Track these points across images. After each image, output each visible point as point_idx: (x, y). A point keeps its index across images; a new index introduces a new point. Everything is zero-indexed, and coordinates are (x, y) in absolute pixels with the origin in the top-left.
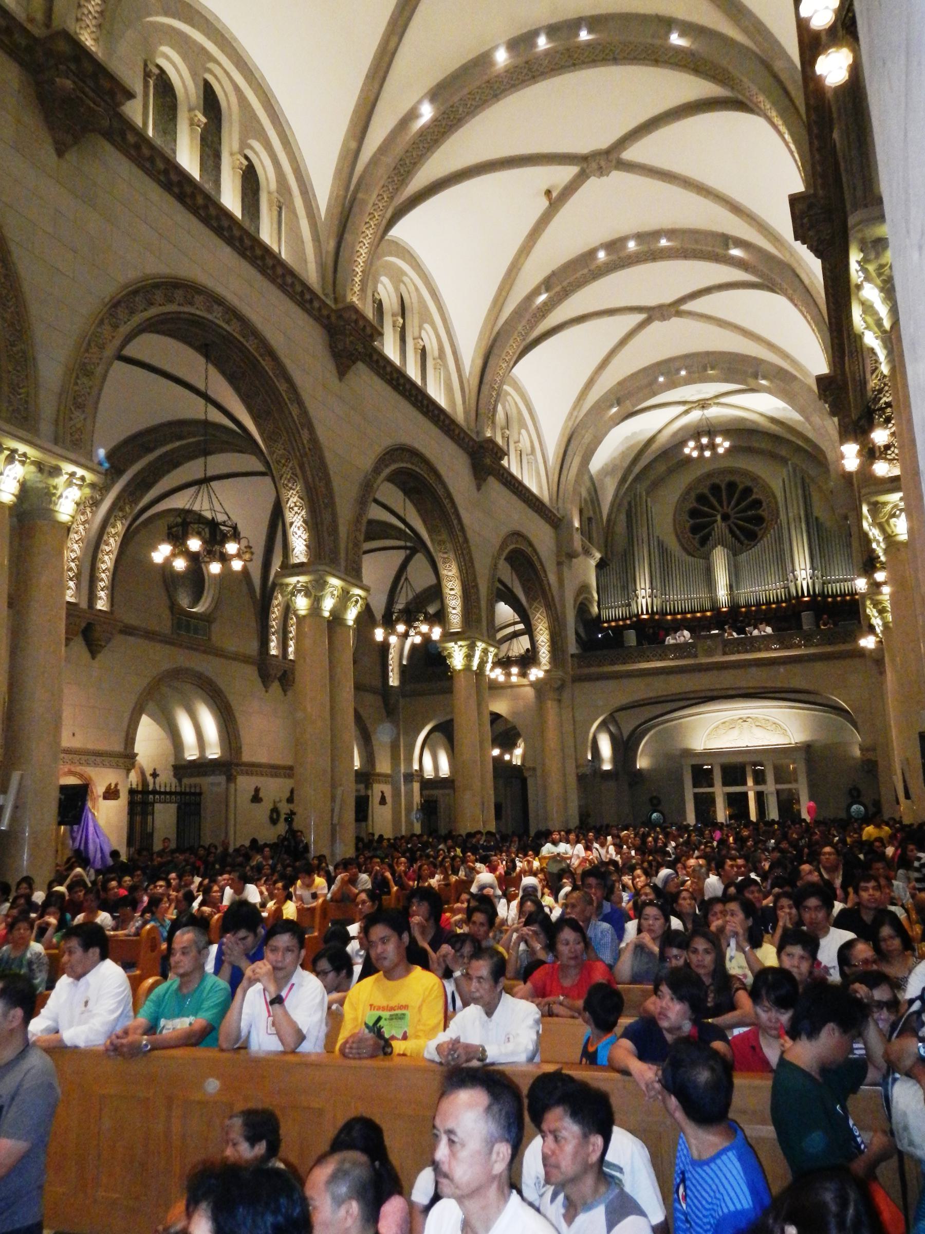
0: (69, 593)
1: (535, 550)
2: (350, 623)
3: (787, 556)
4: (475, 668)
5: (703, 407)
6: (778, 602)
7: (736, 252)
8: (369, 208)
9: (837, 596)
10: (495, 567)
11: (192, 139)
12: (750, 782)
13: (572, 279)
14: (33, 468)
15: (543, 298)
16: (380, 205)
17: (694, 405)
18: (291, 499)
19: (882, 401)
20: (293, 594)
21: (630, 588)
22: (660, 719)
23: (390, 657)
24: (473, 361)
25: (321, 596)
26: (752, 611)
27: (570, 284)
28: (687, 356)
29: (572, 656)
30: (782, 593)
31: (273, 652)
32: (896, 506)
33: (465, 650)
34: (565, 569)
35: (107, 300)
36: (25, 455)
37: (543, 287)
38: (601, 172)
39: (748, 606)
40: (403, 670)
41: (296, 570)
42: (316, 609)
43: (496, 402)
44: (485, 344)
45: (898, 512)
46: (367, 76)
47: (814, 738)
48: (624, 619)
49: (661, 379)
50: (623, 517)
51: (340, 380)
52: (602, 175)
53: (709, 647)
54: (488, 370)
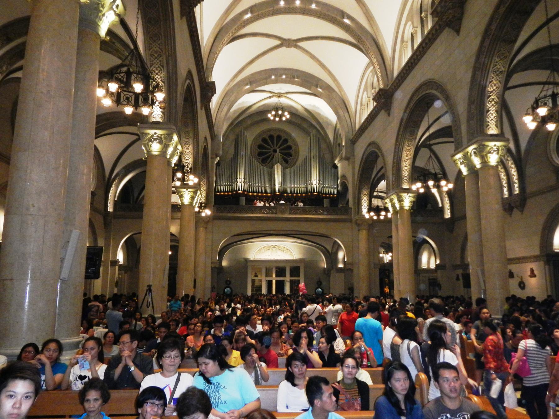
3: (308, 172)
5: (279, 97)
6: (301, 194)
7: (346, 21)
9: (327, 194)
12: (274, 276)
13: (263, 11)
15: (249, 15)
19: (491, 98)
23: (110, 195)
24: (208, 39)
25: (169, 145)
26: (293, 196)
28: (286, 69)
30: (304, 190)
32: (492, 148)
33: (191, 194)
37: (249, 10)
39: (288, 193)
40: (116, 203)
41: (155, 126)
42: (163, 152)
44: (217, 30)
45: (492, 151)
47: (304, 257)
48: (228, 192)
53: (283, 209)
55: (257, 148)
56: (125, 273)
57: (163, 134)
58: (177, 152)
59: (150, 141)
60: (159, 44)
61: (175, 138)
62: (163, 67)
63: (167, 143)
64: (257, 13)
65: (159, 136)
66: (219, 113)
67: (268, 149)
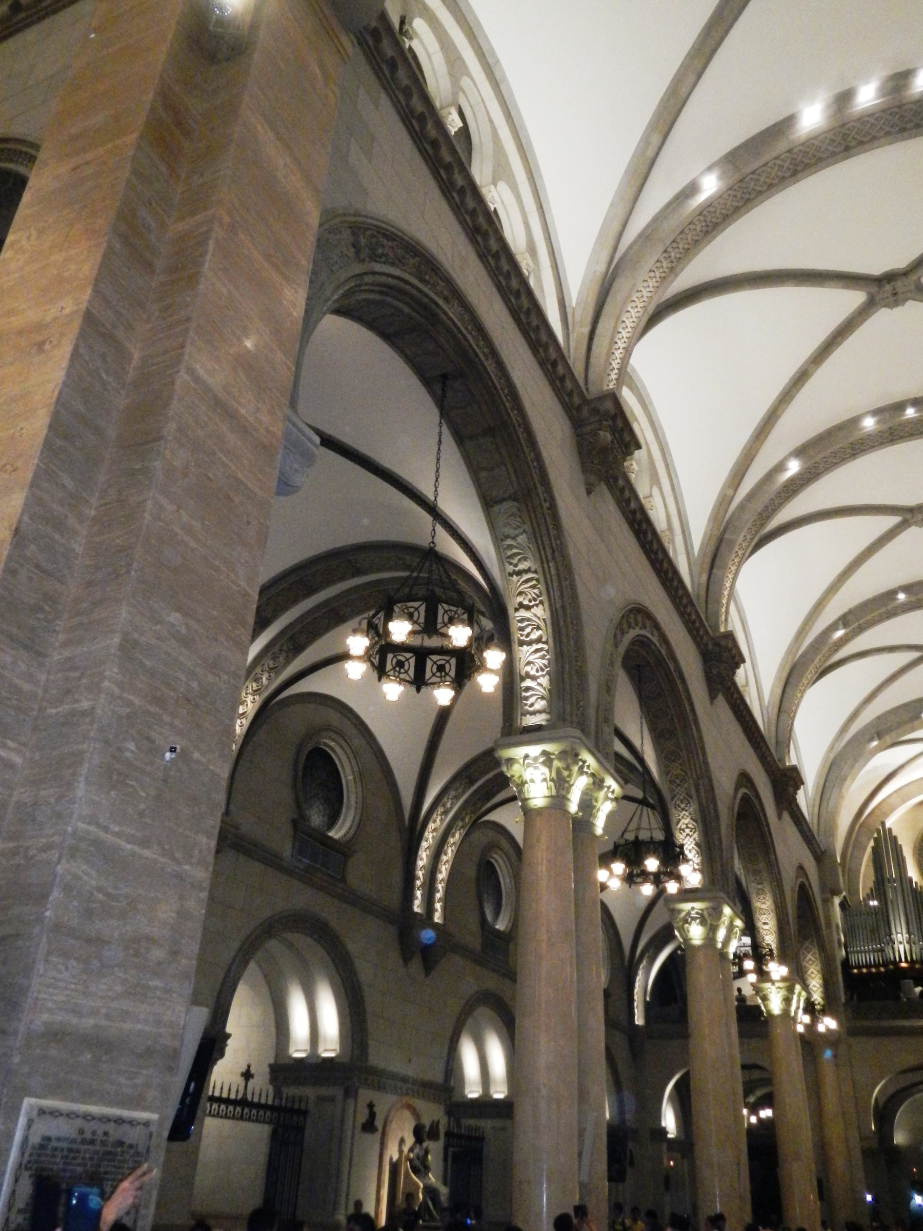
2: (731, 957)
8: (736, 549)
14: (591, 780)
15: (840, 633)
18: (683, 821)
21: (882, 932)
23: (636, 991)
24: (772, 691)
29: (845, 1005)
33: (783, 993)
37: (840, 622)
40: (648, 1007)
42: (710, 939)
44: (785, 674)
48: (877, 966)
51: (712, 703)
54: (784, 700)
57: (706, 909)
58: (735, 931)
59: (686, 922)
60: (681, 765)
61: (727, 911)
62: (691, 798)
63: (715, 924)
64: (857, 623)
65: (700, 912)
66: (824, 804)
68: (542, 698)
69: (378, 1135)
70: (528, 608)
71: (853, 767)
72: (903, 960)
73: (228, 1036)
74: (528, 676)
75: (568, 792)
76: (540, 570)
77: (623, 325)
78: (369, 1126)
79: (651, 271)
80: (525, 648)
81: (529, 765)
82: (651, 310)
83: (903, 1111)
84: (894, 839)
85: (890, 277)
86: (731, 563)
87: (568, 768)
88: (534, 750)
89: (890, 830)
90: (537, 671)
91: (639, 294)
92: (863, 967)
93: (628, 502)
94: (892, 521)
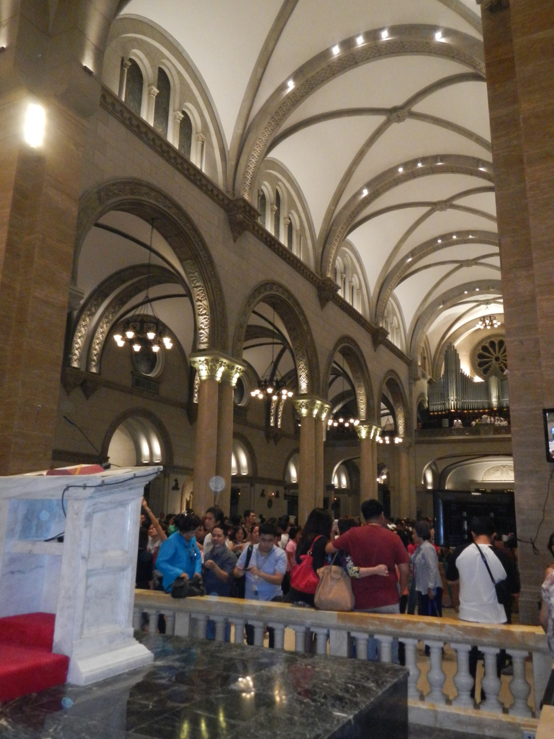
0: (195, 399)
1: (399, 378)
4: (371, 438)
8: (338, 234)
10: (381, 389)
11: (272, 218)
13: (425, 251)
14: (226, 367)
16: (342, 232)
17: (482, 303)
20: (300, 407)
22: (458, 464)
24: (375, 289)
27: (424, 253)
31: (272, 425)
33: (367, 429)
34: (413, 386)
35: (248, 296)
36: (225, 363)
37: (410, 255)
38: (442, 209)
43: (385, 308)
46: (341, 180)
48: (441, 411)
49: (466, 292)
50: (443, 357)
51: (322, 310)
52: (443, 210)
54: (382, 294)
55: (477, 358)
56: (349, 496)
67: (488, 357)
68: (206, 337)
69: (180, 491)
70: (201, 301)
71: (430, 319)
72: (453, 408)
73: (109, 458)
74: (202, 328)
75: (216, 373)
76: (204, 286)
77: (253, 157)
78: (176, 488)
79: (266, 128)
80: (200, 317)
81: (201, 364)
82: (268, 145)
83: (451, 475)
84: (456, 351)
85: (394, 110)
86: (334, 242)
87: (215, 365)
88: (203, 359)
89: (454, 346)
90: (205, 326)
91: (260, 140)
92: (436, 412)
93: (262, 235)
94: (426, 209)
